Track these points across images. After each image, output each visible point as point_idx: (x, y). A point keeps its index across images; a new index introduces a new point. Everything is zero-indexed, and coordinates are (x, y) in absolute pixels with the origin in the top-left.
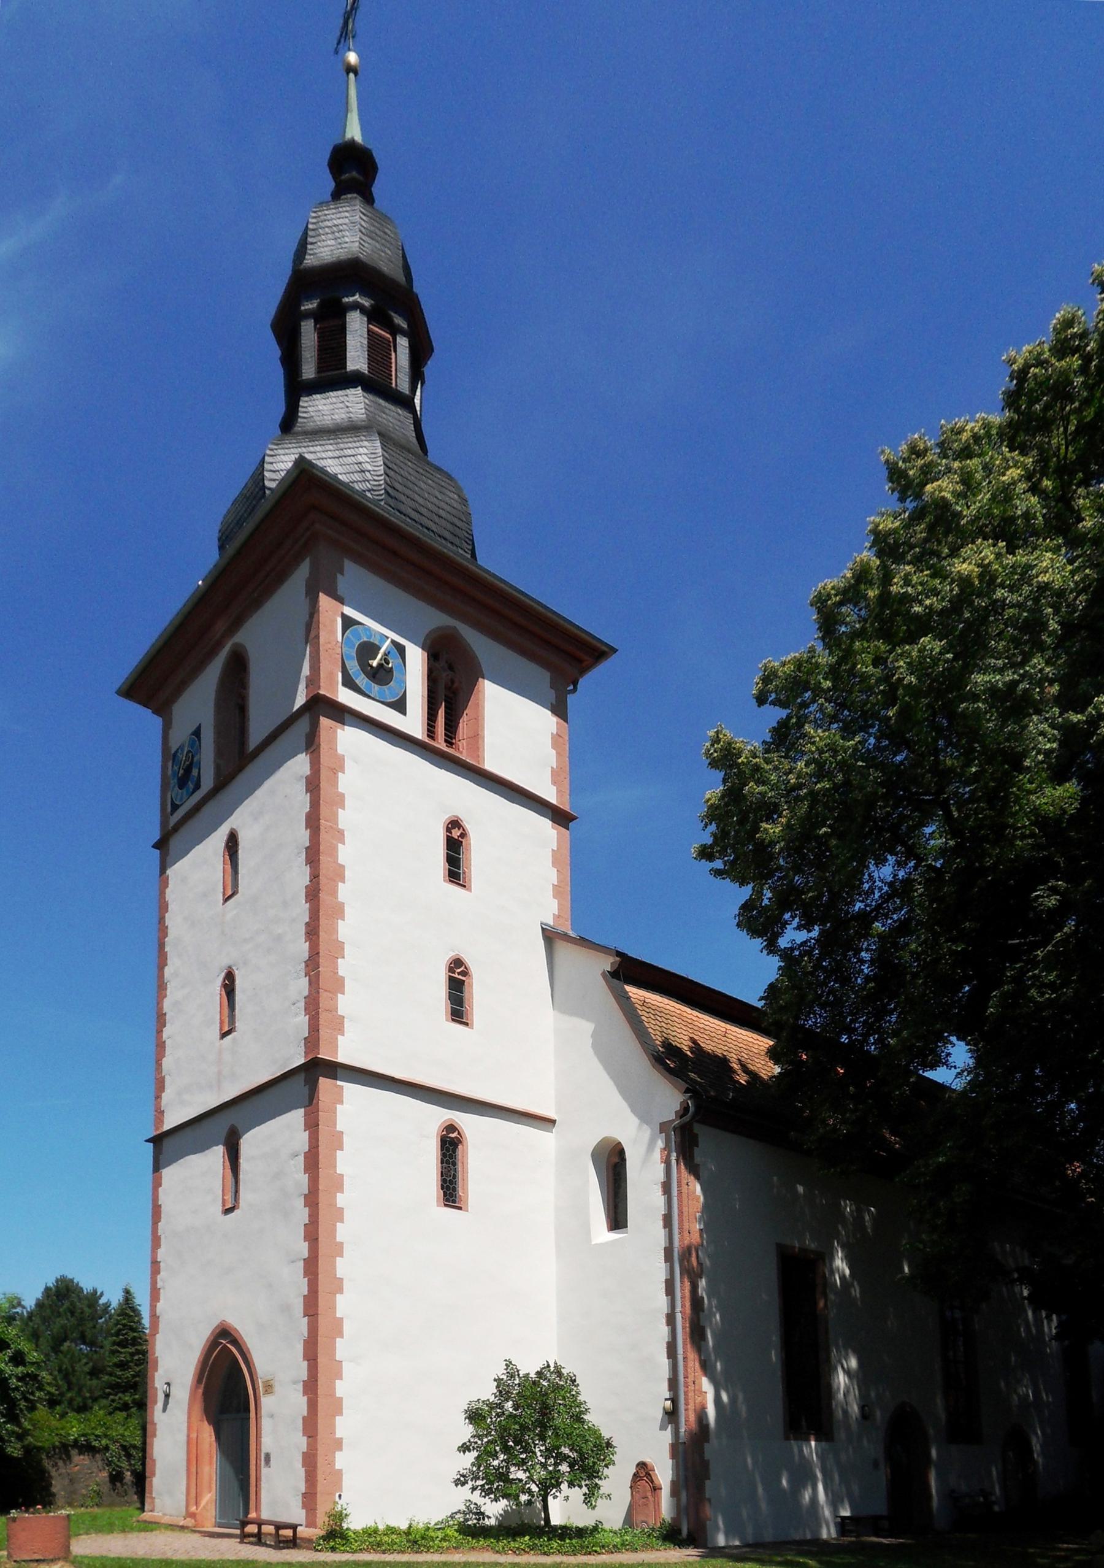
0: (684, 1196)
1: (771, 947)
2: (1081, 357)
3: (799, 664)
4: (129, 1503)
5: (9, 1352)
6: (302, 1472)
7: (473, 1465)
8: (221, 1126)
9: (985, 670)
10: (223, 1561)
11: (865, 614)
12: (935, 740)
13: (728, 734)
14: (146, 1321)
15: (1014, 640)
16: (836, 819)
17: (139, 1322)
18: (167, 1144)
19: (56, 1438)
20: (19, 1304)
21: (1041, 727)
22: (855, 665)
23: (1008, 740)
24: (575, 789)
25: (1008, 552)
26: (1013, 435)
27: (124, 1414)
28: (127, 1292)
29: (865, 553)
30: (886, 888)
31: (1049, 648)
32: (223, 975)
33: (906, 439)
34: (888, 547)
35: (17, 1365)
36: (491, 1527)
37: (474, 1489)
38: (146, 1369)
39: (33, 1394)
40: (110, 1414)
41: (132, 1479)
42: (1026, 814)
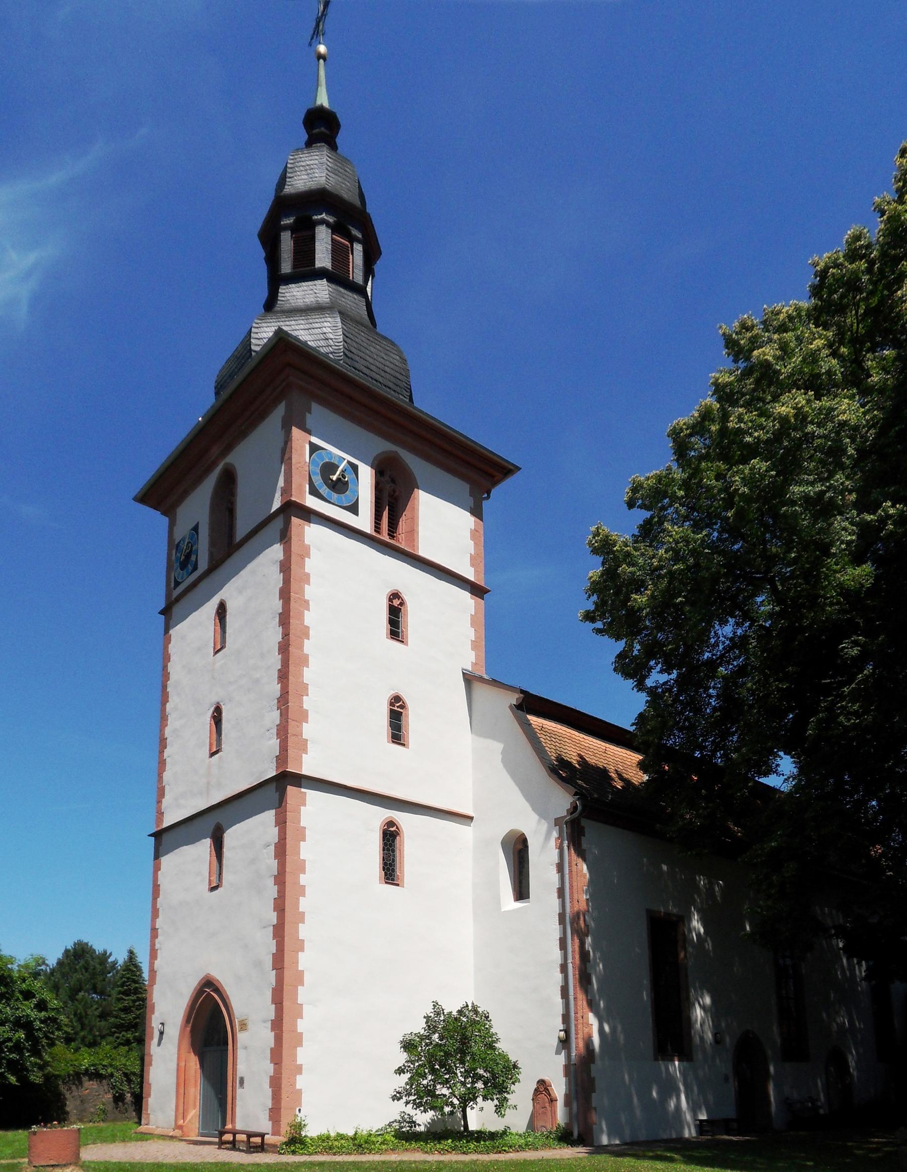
0: (574, 873)
1: (640, 686)
2: (867, 262)
3: (659, 479)
4: (129, 1119)
5: (35, 1001)
6: (269, 1092)
7: (407, 1084)
8: (209, 823)
9: (800, 483)
10: (205, 1163)
11: (709, 443)
12: (764, 534)
13: (605, 529)
14: (146, 975)
15: (821, 461)
16: (688, 591)
17: (140, 976)
18: (166, 838)
19: (71, 1068)
20: (44, 963)
21: (843, 524)
22: (701, 480)
23: (818, 534)
24: (488, 570)
25: (816, 399)
26: (819, 316)
27: (126, 1048)
28: (131, 952)
29: (708, 399)
30: (728, 642)
31: (848, 467)
32: (212, 709)
33: (737, 318)
34: (726, 395)
35: (40, 1011)
36: (421, 1133)
37: (407, 1103)
38: (145, 1013)
39: (53, 1033)
40: (115, 1048)
41: (131, 1099)
42: (834, 588)
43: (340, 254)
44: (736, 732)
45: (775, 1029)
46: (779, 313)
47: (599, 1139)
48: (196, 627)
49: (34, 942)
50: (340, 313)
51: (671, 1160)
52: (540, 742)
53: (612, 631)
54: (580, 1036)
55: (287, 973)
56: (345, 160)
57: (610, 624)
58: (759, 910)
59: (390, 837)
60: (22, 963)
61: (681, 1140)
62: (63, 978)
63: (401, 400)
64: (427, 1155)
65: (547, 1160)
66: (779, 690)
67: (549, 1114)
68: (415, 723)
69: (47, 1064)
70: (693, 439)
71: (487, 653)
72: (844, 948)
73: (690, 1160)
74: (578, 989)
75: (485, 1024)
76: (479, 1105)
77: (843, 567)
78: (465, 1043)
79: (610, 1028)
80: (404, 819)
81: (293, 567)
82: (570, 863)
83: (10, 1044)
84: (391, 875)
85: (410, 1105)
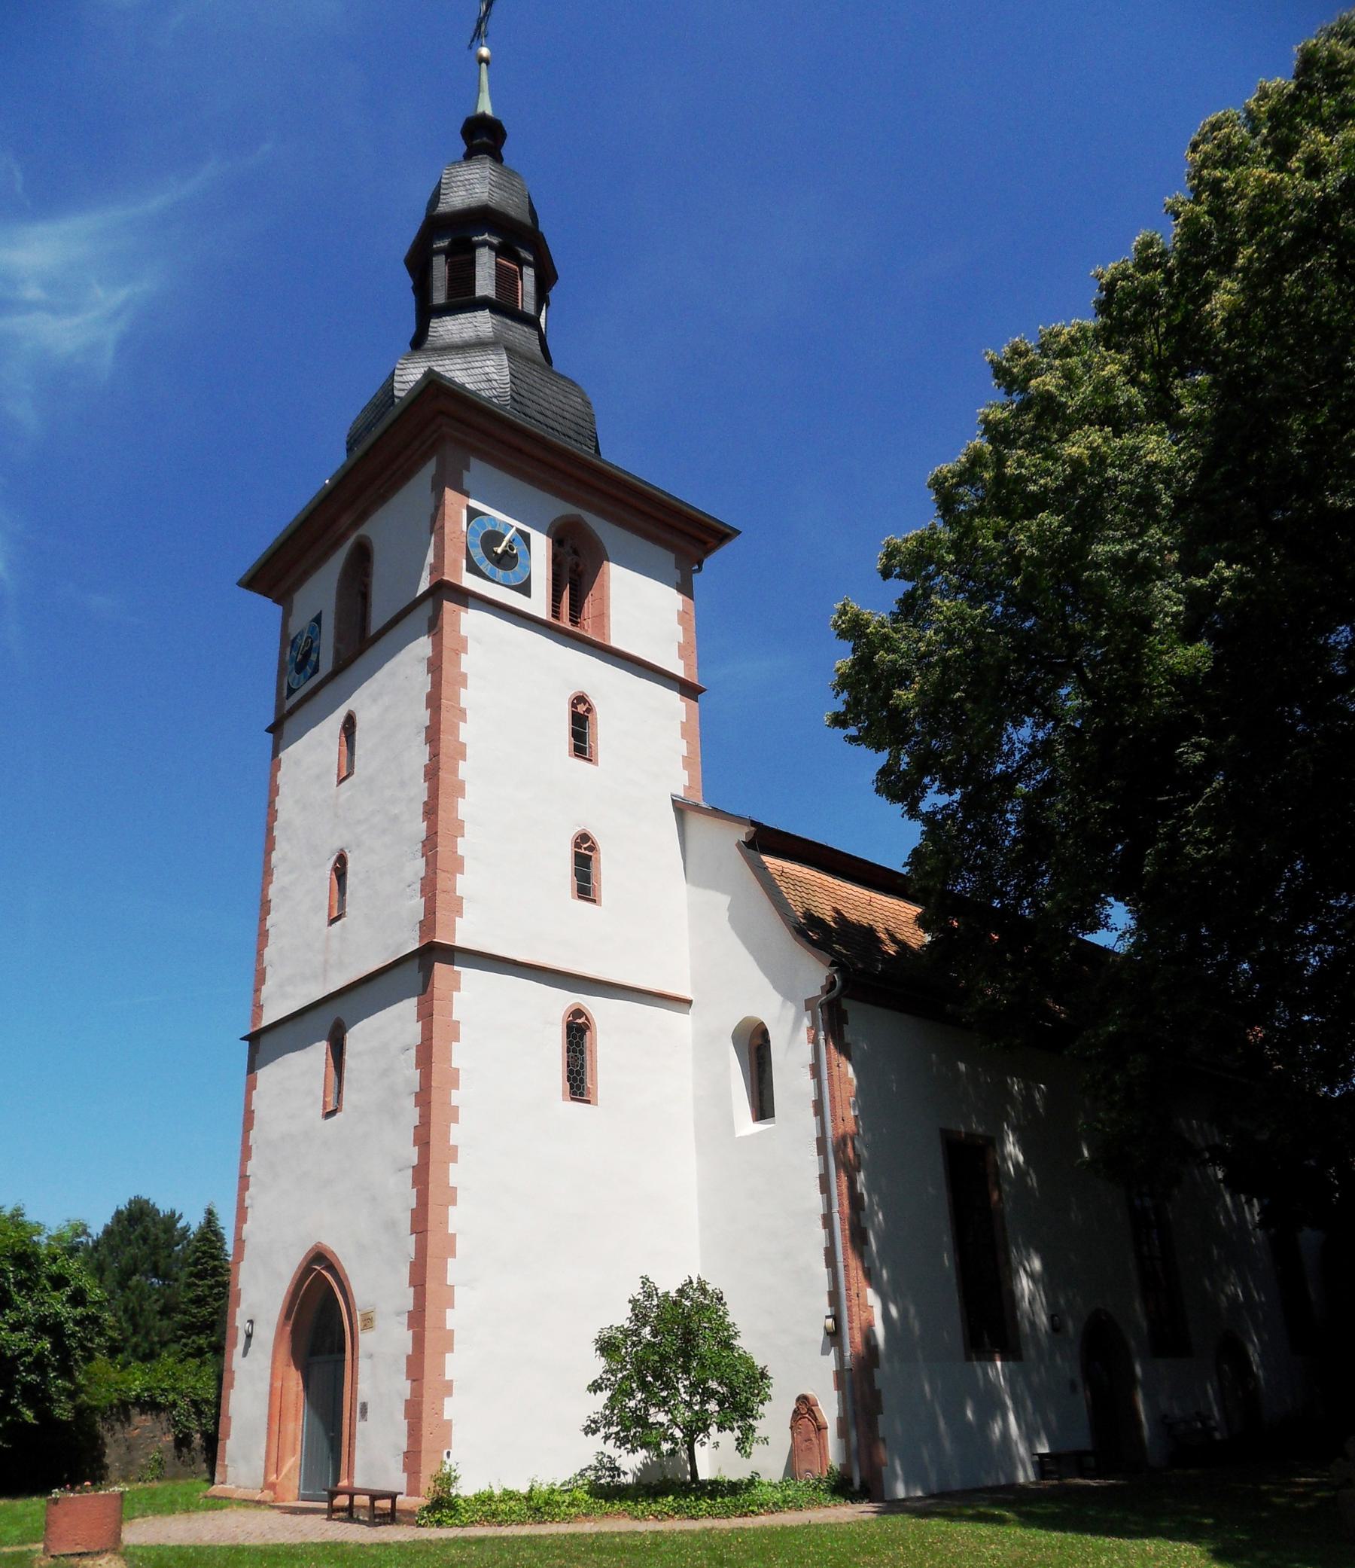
0: (836, 1079)
1: (913, 812)
2: (1163, 271)
3: (921, 541)
4: (196, 1474)
5: (68, 1291)
6: (404, 1425)
7: (606, 1407)
8: (324, 1020)
9: (1105, 541)
10: (306, 1544)
11: (984, 494)
12: (1062, 606)
13: (855, 606)
14: (229, 1247)
15: (1128, 513)
16: (968, 683)
17: (222, 1248)
18: (265, 1041)
19: (115, 1395)
20: (85, 1232)
21: (1166, 591)
22: (976, 540)
23: (1134, 604)
25: (1115, 436)
26: (1111, 335)
27: (197, 1361)
28: (210, 1213)
29: (977, 440)
30: (1026, 750)
31: (1164, 519)
32: (334, 858)
33: (1007, 341)
34: (999, 435)
35: (75, 1307)
36: (628, 1486)
37: (607, 1438)
38: (226, 1305)
39: (91, 1340)
40: (181, 1361)
41: (201, 1444)
42: (1161, 674)
43: (506, 281)
44: (1046, 871)
45: (1137, 1305)
46: (1059, 334)
47: (893, 1491)
48: (314, 748)
49: (69, 1202)
50: (506, 348)
51: (1001, 1521)
52: (781, 892)
53: (871, 738)
54: (856, 1325)
55: (431, 1238)
56: (512, 173)
57: (868, 729)
58: (1100, 1126)
59: (577, 1031)
60: (54, 1233)
61: (1012, 1487)
62: (111, 1254)
63: (585, 451)
64: (637, 1522)
65: (817, 1526)
66: (1101, 812)
67: (816, 1450)
68: (607, 871)
69: (80, 1389)
70: (961, 490)
71: (705, 771)
72: (1225, 1180)
73: (1029, 1520)
74: (850, 1251)
75: (718, 1310)
76: (713, 1439)
77: (1171, 647)
78: (689, 1341)
79: (899, 1311)
80: (596, 1007)
81: (446, 665)
82: (829, 1063)
83: (28, 1359)
84: (579, 1087)
85: (611, 1442)
